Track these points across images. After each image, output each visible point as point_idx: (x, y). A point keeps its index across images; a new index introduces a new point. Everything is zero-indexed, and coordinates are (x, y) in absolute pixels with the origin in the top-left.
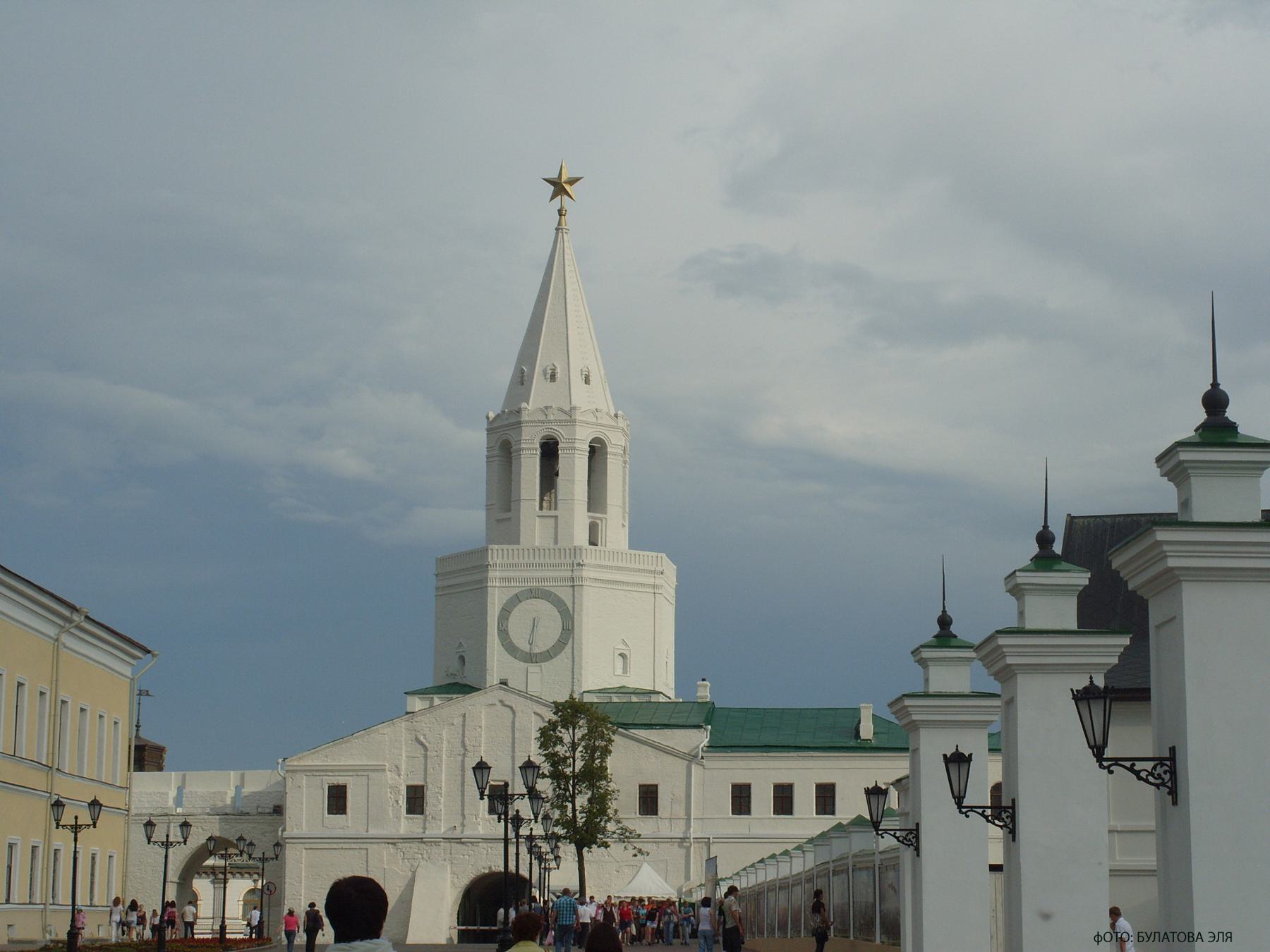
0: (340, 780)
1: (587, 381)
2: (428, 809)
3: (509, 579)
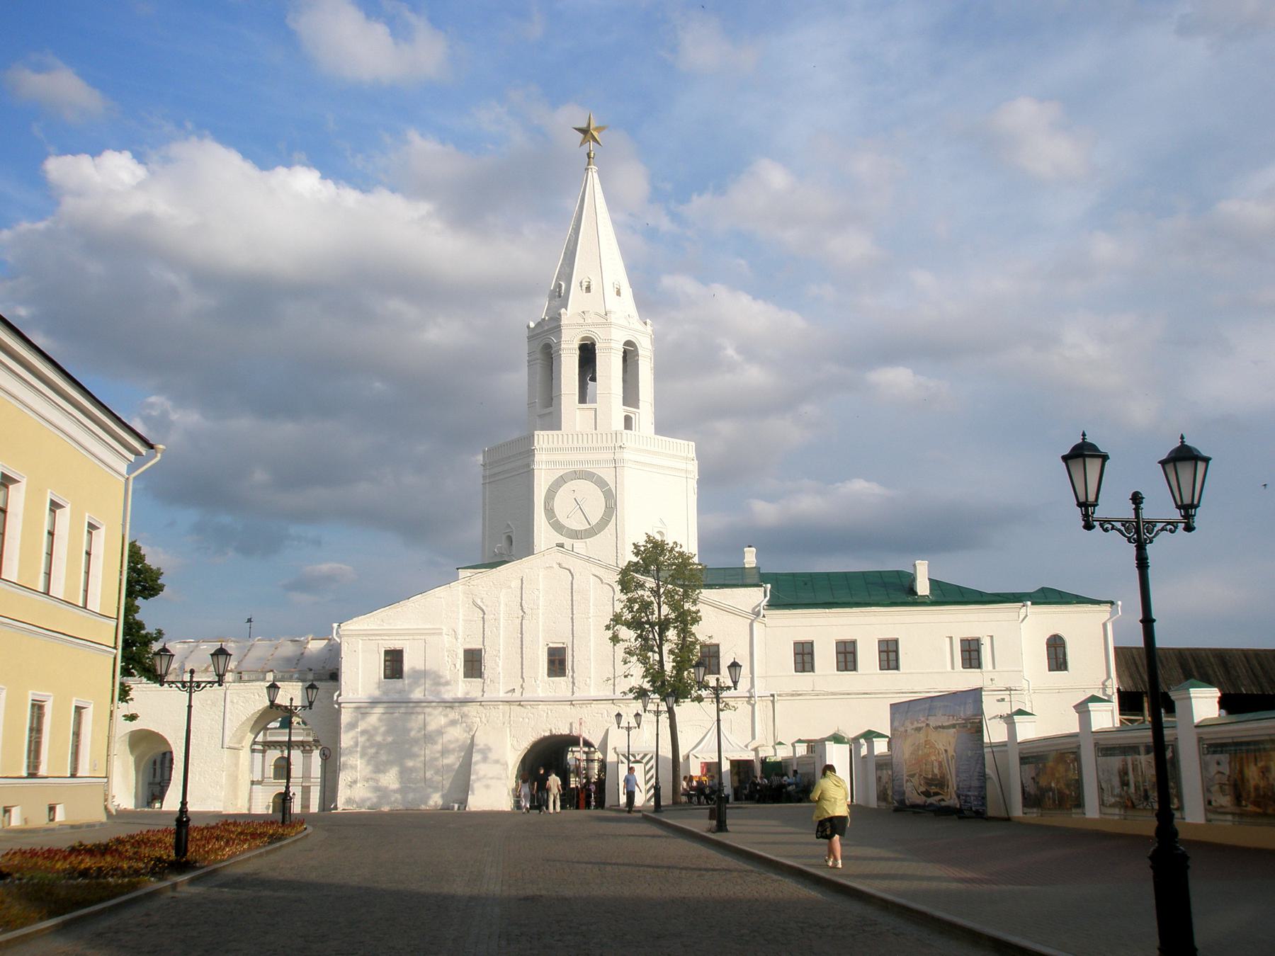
1: (618, 293)
3: (555, 463)
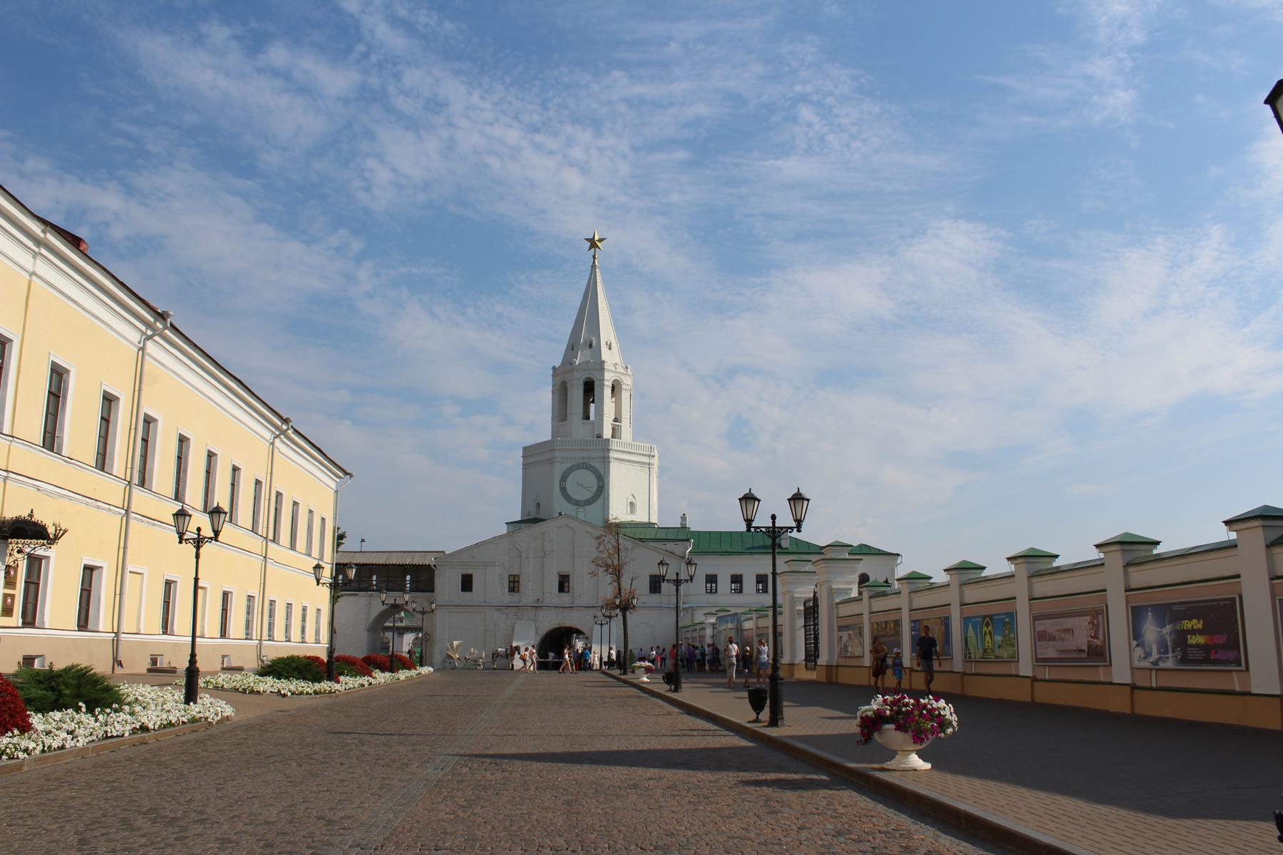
0: (469, 572)
2: (521, 589)
